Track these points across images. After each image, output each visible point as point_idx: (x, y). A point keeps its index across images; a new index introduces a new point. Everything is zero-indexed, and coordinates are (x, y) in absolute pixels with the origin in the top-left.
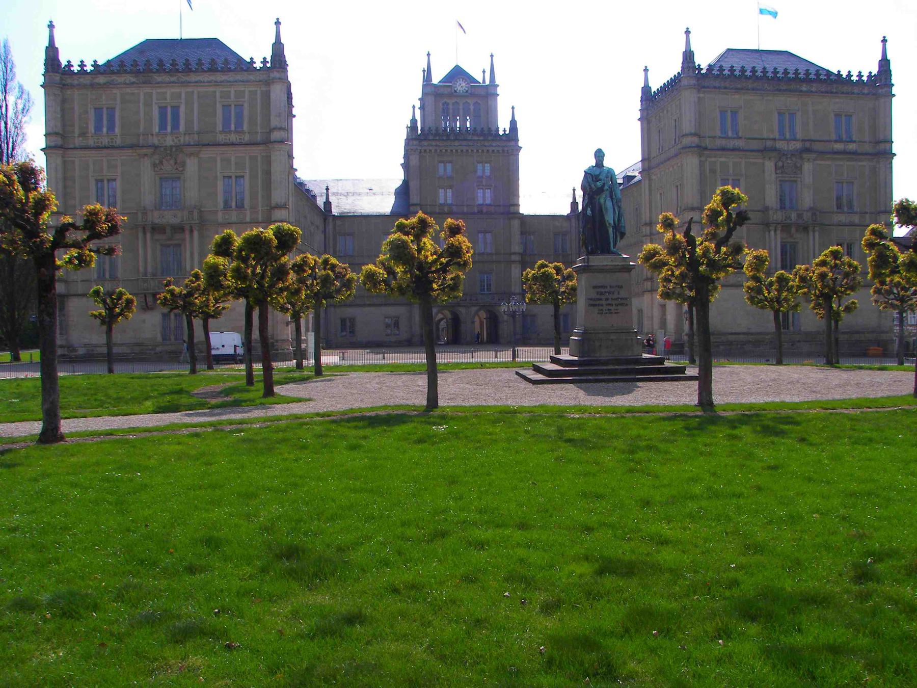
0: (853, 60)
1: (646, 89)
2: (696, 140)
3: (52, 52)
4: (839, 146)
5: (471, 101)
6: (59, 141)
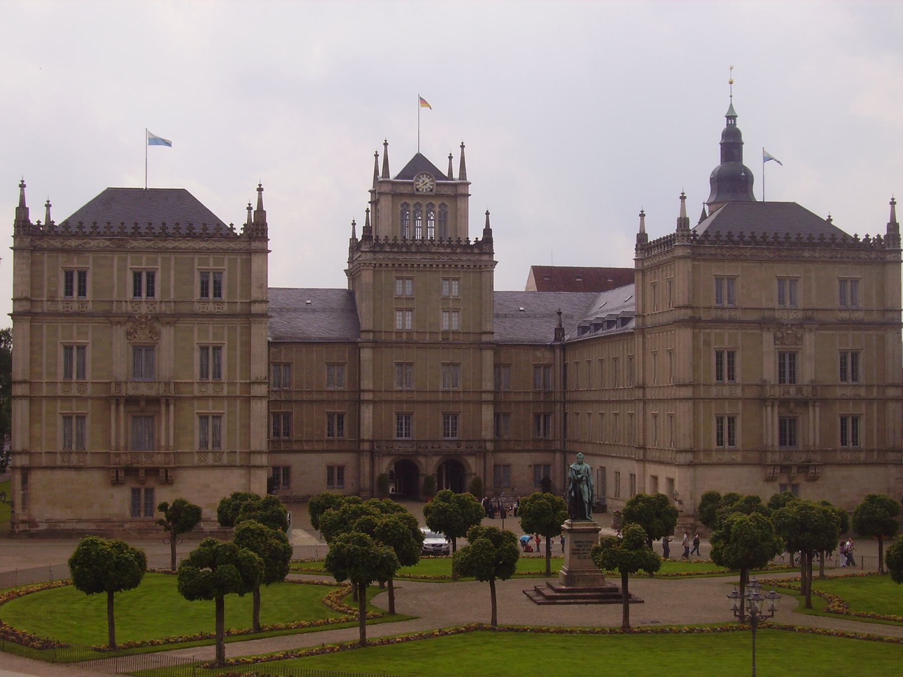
1: (642, 237)
2: (689, 312)
3: (22, 211)
4: (845, 315)
5: (437, 203)
6: (26, 306)
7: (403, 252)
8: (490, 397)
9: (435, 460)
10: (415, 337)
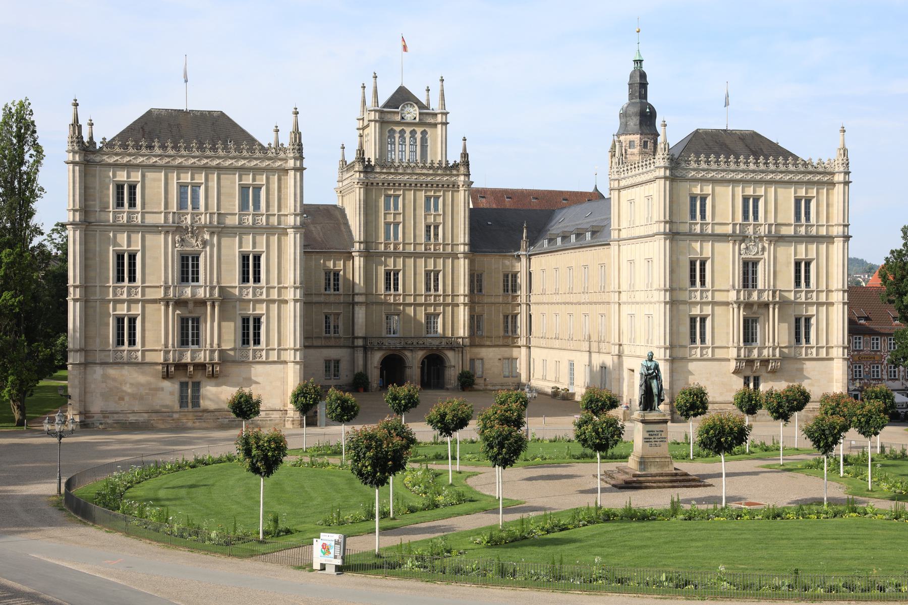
5: (419, 130)
7: (391, 173)
9: (420, 355)
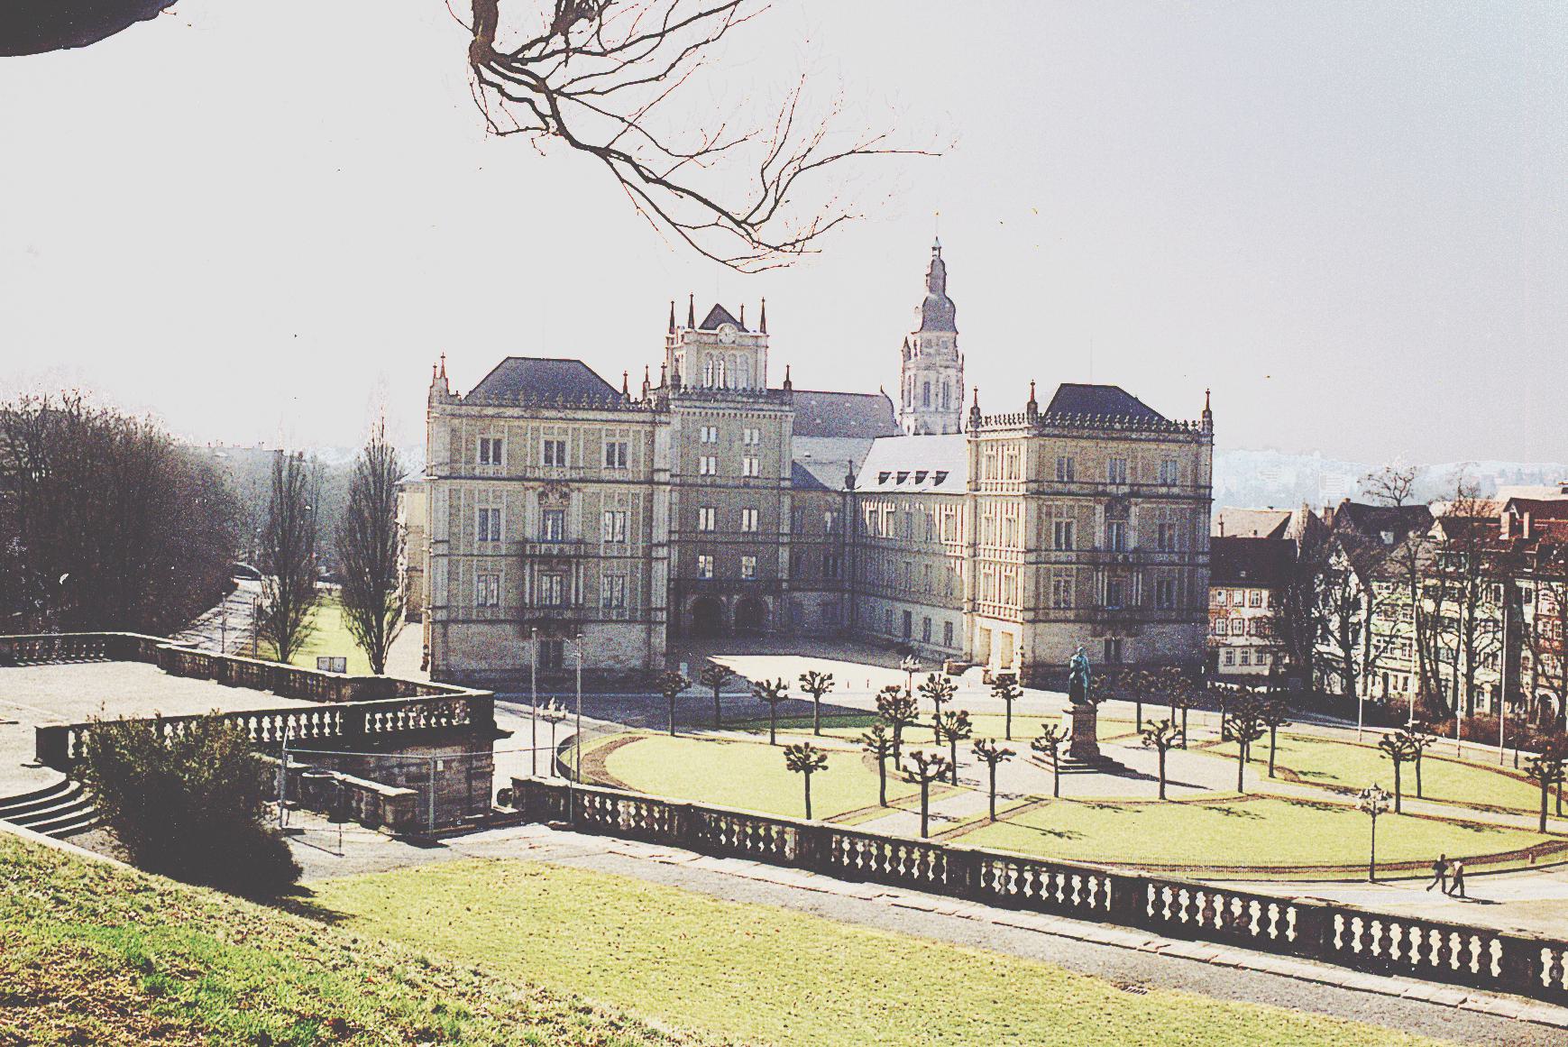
0: (1178, 408)
8: (786, 539)
10: (718, 481)
